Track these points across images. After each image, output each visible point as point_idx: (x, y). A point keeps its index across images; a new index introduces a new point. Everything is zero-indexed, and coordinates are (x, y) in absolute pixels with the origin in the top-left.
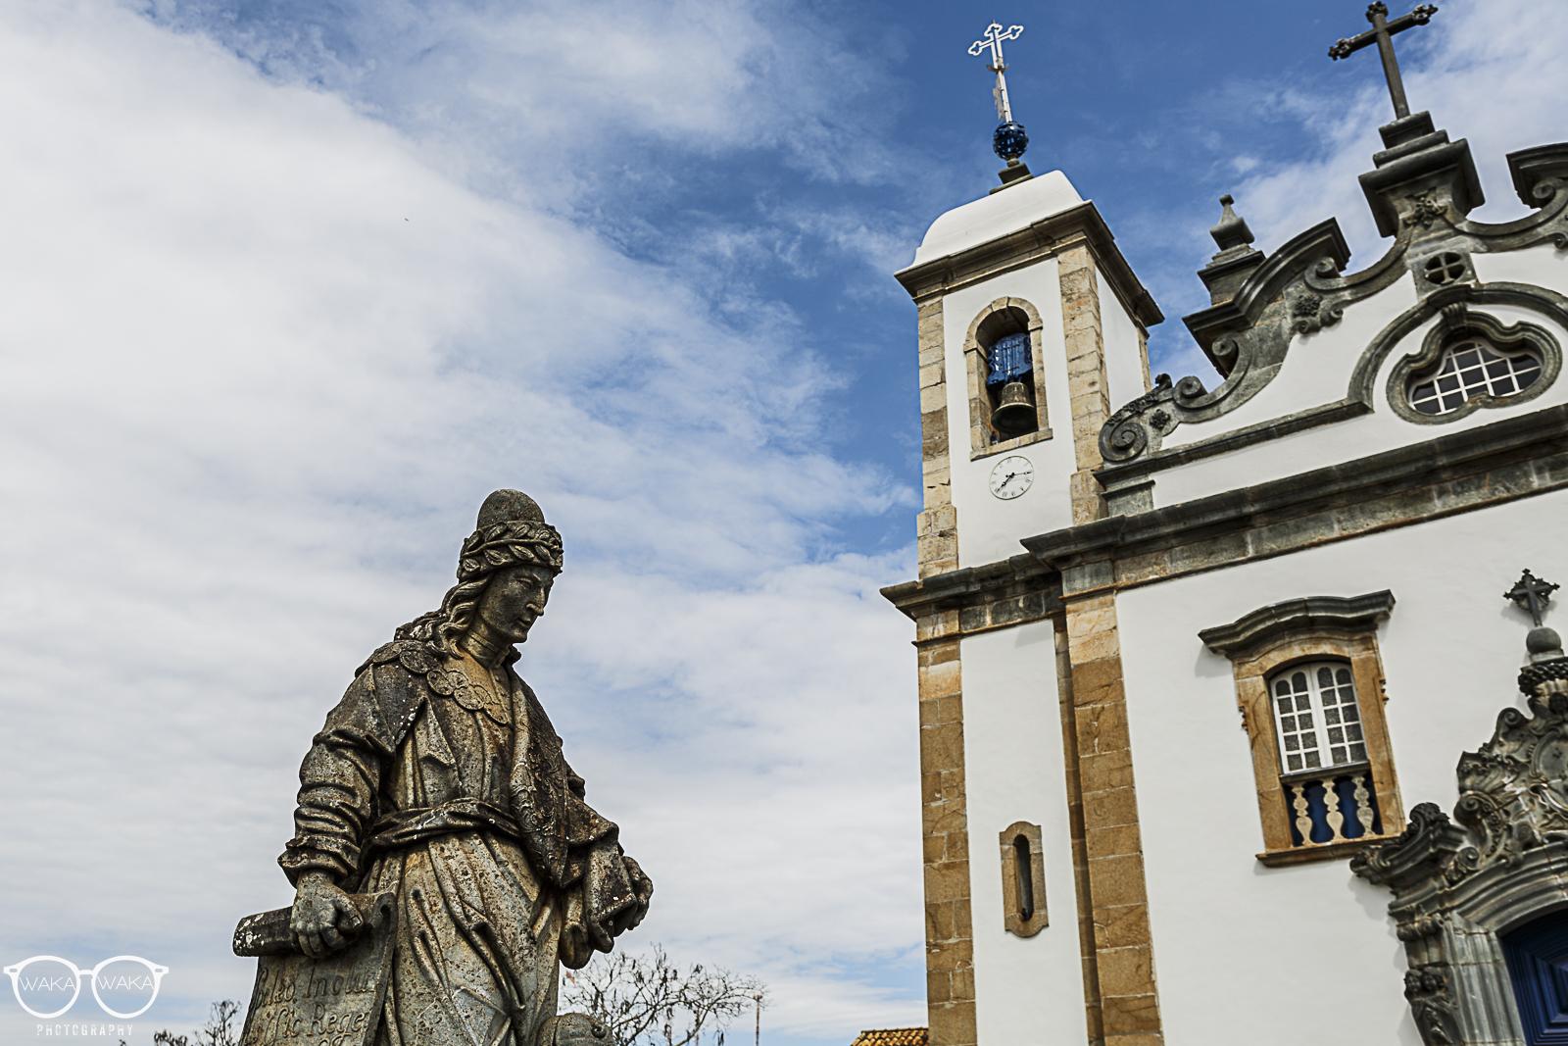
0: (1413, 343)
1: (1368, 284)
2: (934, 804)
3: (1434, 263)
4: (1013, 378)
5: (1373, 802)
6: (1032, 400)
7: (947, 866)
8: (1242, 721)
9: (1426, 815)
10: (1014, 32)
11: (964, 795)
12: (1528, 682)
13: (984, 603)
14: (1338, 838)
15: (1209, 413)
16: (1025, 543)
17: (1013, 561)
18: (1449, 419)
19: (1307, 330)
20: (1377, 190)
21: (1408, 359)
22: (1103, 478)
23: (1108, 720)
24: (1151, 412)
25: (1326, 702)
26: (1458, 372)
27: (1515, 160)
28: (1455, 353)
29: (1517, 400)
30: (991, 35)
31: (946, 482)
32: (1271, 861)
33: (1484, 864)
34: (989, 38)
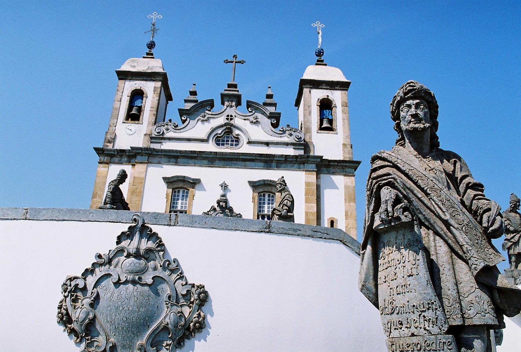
0: (219, 131)
3: (228, 116)
4: (136, 106)
12: (218, 202)
13: (117, 157)
16: (131, 147)
17: (127, 150)
20: (223, 96)
23: (138, 190)
24: (166, 126)
25: (182, 197)
26: (225, 139)
27: (248, 102)
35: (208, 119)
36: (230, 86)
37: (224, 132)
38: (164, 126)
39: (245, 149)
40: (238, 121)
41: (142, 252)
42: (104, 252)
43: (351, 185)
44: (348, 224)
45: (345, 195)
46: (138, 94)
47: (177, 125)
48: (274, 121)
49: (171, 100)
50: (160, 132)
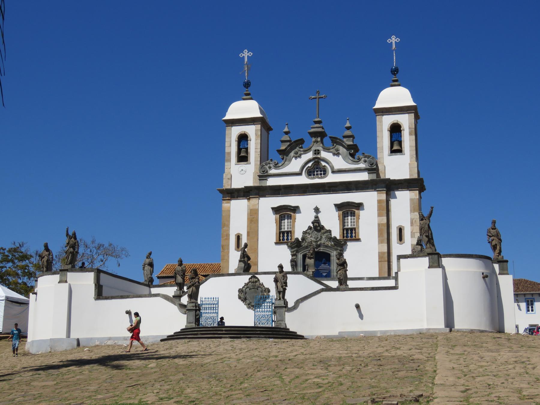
0: (310, 165)
1: (306, 151)
2: (224, 228)
3: (315, 151)
5: (291, 236)
6: (248, 155)
7: (225, 239)
8: (275, 222)
9: (297, 239)
10: (250, 54)
11: (229, 227)
12: (313, 223)
14: (286, 241)
15: (278, 168)
17: (242, 188)
18: (313, 178)
19: (296, 158)
21: (309, 166)
22: (259, 176)
24: (268, 165)
27: (330, 137)
28: (316, 166)
29: (321, 178)
30: (245, 53)
31: (230, 168)
32: (276, 243)
33: (303, 246)
34: (244, 53)
35: (301, 156)
36: (316, 122)
37: (313, 165)
38: (267, 165)
39: (331, 178)
40: (324, 154)
41: (254, 282)
42: (246, 282)
43: (415, 198)
44: (413, 230)
45: (411, 207)
46: (243, 138)
47: (277, 163)
48: (351, 151)
49: (271, 129)
50: (264, 171)
